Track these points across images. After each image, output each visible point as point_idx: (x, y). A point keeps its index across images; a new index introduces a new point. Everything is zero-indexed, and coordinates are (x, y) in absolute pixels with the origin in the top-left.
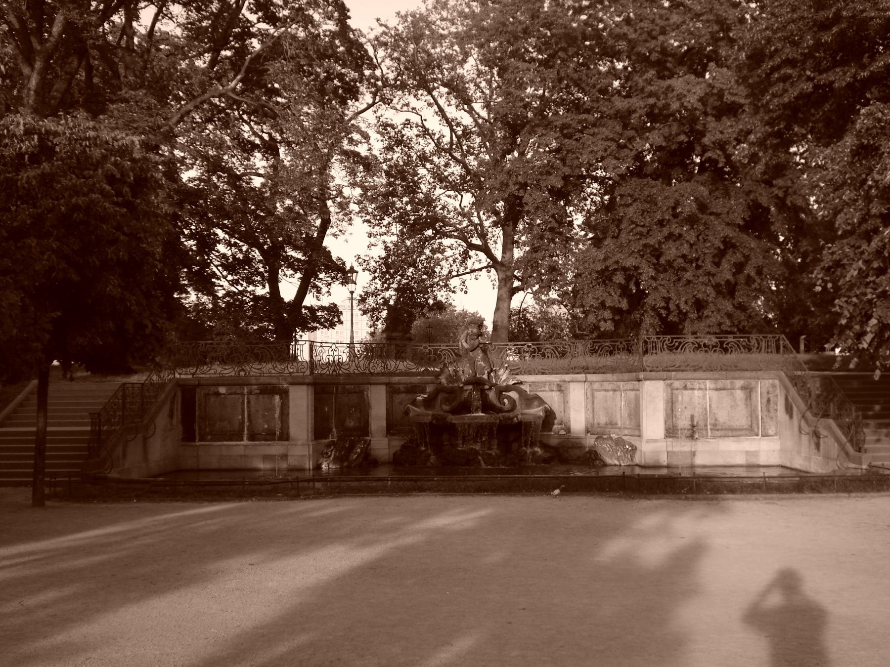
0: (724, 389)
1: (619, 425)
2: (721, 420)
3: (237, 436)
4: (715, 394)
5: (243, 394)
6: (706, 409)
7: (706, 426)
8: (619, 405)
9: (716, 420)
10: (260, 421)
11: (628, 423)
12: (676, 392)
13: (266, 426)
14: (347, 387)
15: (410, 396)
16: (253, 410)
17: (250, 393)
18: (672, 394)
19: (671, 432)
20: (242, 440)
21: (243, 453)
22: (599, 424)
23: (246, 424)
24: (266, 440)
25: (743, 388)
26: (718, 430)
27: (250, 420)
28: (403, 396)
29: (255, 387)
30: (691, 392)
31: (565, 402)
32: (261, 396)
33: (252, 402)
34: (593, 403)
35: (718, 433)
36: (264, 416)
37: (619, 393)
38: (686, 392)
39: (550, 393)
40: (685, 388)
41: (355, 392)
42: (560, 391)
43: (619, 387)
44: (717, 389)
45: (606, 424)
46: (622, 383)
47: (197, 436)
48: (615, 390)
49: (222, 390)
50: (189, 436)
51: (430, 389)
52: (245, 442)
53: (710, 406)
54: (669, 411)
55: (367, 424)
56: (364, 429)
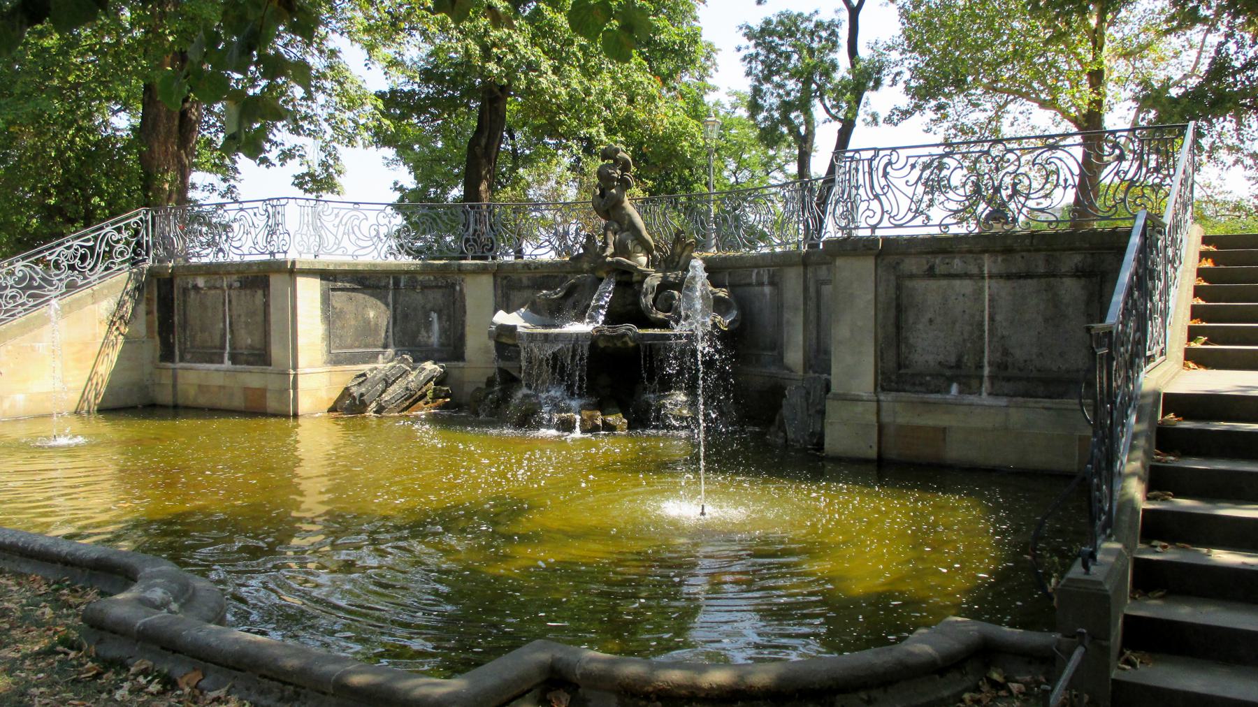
0: (1028, 276)
2: (1019, 354)
3: (215, 357)
4: (1004, 289)
5: (221, 288)
6: (981, 324)
7: (980, 367)
9: (1006, 352)
10: (243, 332)
12: (909, 284)
13: (249, 341)
16: (235, 313)
17: (230, 287)
18: (899, 288)
19: (895, 374)
20: (222, 362)
21: (221, 383)
23: (228, 336)
24: (248, 363)
25: (1078, 273)
26: (1008, 379)
27: (232, 331)
29: (235, 277)
30: (944, 283)
32: (243, 292)
33: (234, 303)
34: (818, 307)
35: (1007, 387)
36: (247, 324)
38: (933, 284)
40: (931, 273)
41: (437, 287)
44: (1009, 277)
47: (177, 352)
49: (201, 282)
50: (167, 354)
52: (227, 364)
53: (992, 319)
54: (891, 330)
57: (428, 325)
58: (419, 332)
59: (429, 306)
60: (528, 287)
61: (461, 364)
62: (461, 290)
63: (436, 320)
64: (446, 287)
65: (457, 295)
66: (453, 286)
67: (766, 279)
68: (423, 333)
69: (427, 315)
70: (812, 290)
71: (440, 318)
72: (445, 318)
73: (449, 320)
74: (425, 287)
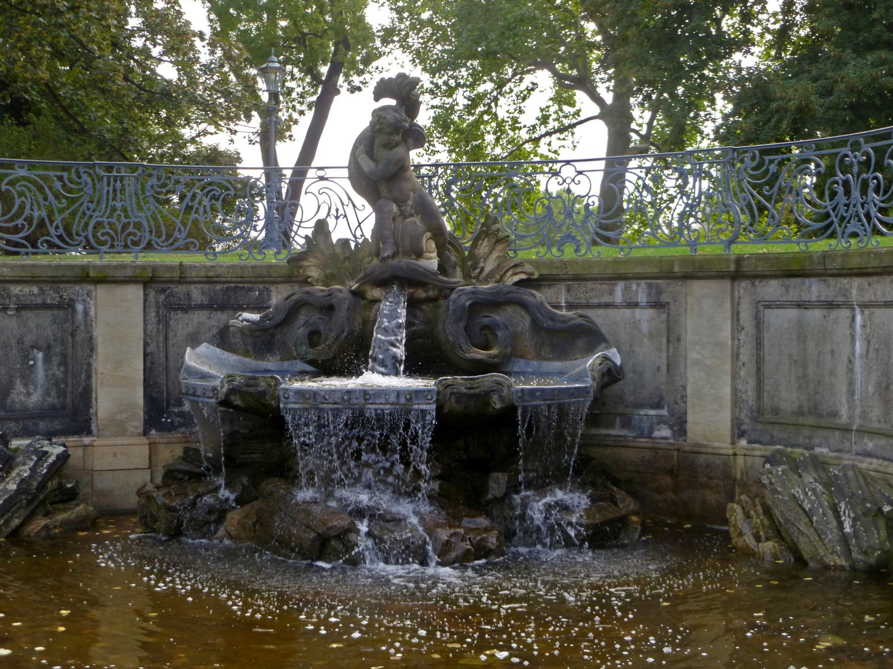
1: (844, 417)
8: (845, 351)
11: (875, 413)
14: (16, 289)
15: (219, 318)
22: (776, 411)
28: (200, 316)
31: (672, 336)
34: (759, 344)
37: (845, 313)
39: (627, 312)
41: (45, 306)
42: (658, 305)
43: (846, 292)
45: (800, 413)
46: (857, 282)
48: (831, 305)
51: (277, 297)
55: (86, 396)
56: (73, 413)
57: (27, 375)
58: (11, 384)
59: (29, 340)
60: (202, 307)
61: (87, 440)
62: (86, 313)
63: (40, 364)
64: (59, 307)
65: (80, 317)
66: (71, 304)
67: (642, 298)
68: (19, 387)
69: (26, 357)
70: (746, 316)
71: (47, 360)
72: (56, 360)
73: (64, 362)
74: (22, 307)
